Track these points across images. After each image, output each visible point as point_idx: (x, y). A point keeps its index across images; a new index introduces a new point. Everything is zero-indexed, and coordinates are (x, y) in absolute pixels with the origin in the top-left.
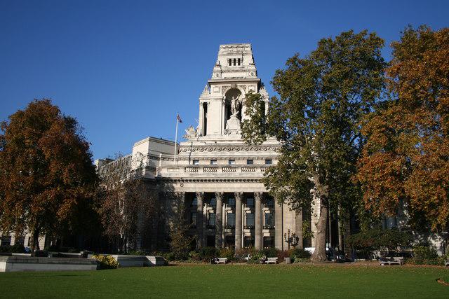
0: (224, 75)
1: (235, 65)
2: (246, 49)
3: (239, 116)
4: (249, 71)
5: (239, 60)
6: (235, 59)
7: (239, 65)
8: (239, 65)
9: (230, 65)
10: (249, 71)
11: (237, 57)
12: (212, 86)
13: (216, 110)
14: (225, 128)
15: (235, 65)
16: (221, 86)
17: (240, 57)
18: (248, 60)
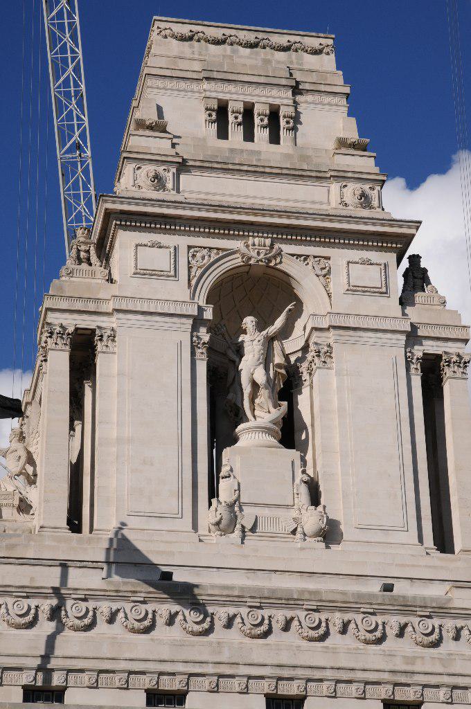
0: (196, 186)
1: (249, 136)
2: (310, 61)
3: (290, 433)
4: (341, 177)
5: (274, 115)
6: (248, 112)
7: (275, 139)
8: (275, 139)
9: (223, 134)
10: (341, 177)
11: (262, 100)
12: (125, 242)
13: (149, 378)
14: (213, 493)
15: (249, 136)
16: (182, 241)
17: (282, 98)
18: (327, 123)
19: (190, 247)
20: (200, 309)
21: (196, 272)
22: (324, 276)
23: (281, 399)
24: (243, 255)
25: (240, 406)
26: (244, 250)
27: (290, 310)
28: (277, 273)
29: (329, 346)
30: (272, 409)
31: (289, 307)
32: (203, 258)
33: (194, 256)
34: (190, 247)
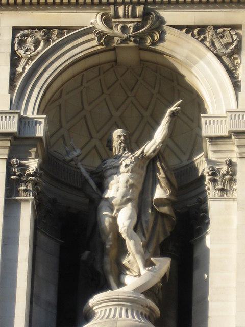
19: (16, 30)
20: (23, 121)
21: (24, 68)
22: (230, 56)
23: (163, 251)
24: (100, 35)
25: (99, 270)
26: (101, 26)
27: (173, 114)
28: (158, 58)
29: (230, 164)
30: (144, 271)
31: (173, 108)
32: (37, 44)
33: (22, 43)
34: (16, 30)
